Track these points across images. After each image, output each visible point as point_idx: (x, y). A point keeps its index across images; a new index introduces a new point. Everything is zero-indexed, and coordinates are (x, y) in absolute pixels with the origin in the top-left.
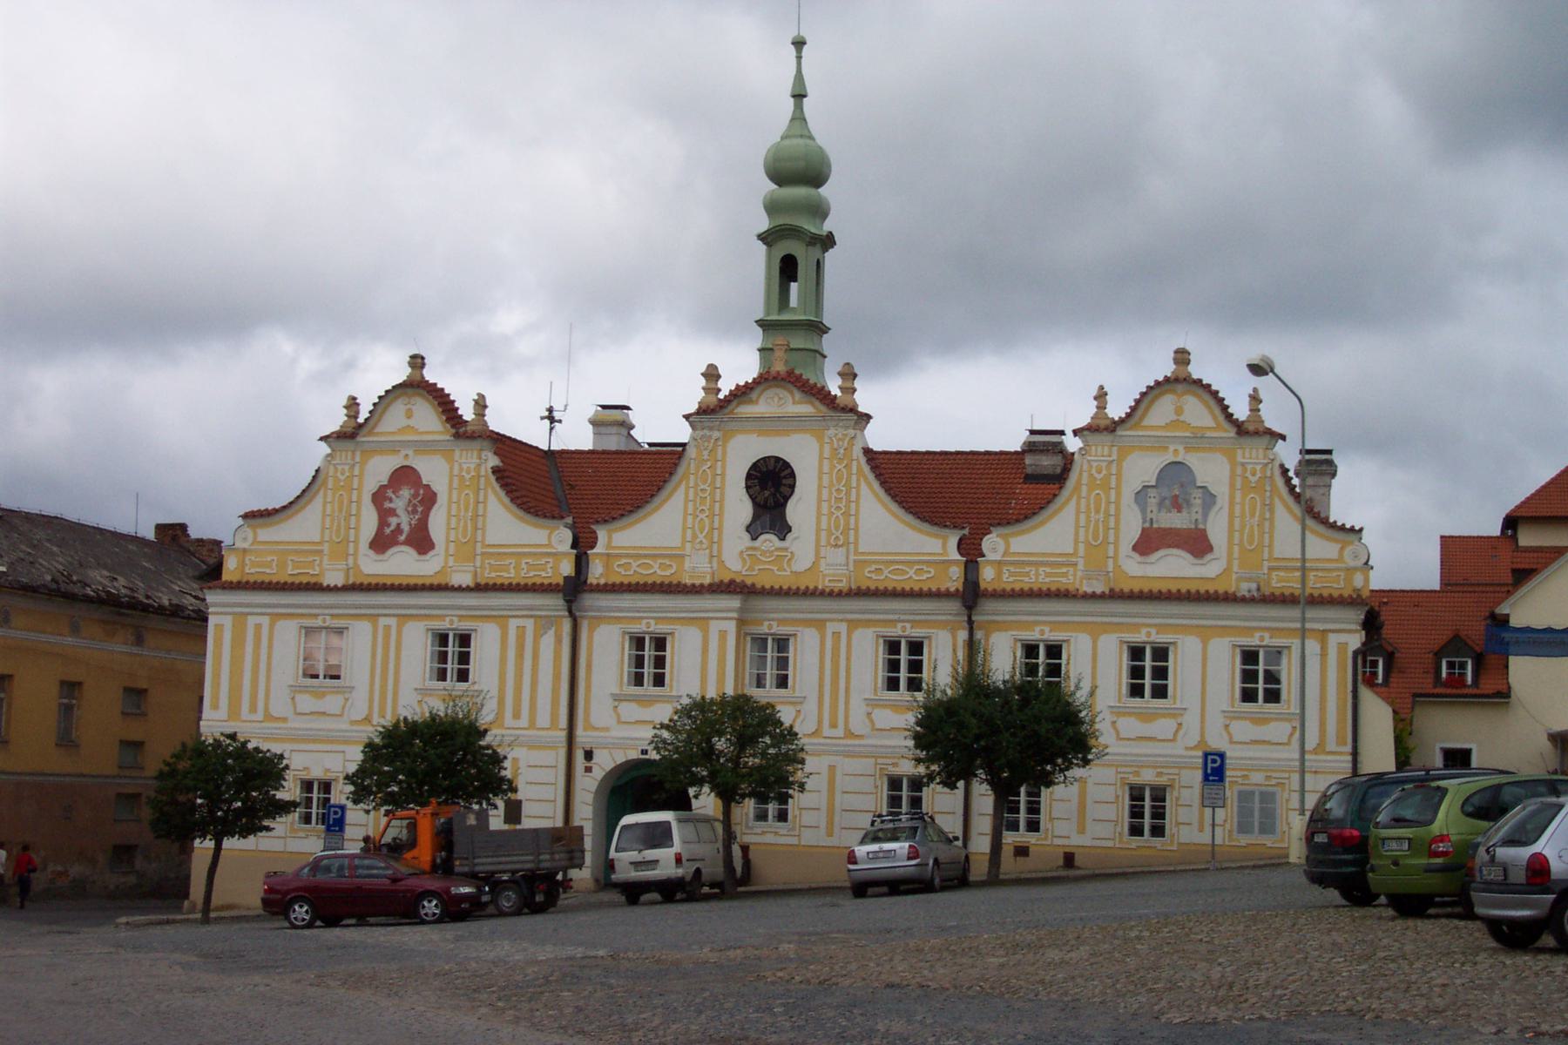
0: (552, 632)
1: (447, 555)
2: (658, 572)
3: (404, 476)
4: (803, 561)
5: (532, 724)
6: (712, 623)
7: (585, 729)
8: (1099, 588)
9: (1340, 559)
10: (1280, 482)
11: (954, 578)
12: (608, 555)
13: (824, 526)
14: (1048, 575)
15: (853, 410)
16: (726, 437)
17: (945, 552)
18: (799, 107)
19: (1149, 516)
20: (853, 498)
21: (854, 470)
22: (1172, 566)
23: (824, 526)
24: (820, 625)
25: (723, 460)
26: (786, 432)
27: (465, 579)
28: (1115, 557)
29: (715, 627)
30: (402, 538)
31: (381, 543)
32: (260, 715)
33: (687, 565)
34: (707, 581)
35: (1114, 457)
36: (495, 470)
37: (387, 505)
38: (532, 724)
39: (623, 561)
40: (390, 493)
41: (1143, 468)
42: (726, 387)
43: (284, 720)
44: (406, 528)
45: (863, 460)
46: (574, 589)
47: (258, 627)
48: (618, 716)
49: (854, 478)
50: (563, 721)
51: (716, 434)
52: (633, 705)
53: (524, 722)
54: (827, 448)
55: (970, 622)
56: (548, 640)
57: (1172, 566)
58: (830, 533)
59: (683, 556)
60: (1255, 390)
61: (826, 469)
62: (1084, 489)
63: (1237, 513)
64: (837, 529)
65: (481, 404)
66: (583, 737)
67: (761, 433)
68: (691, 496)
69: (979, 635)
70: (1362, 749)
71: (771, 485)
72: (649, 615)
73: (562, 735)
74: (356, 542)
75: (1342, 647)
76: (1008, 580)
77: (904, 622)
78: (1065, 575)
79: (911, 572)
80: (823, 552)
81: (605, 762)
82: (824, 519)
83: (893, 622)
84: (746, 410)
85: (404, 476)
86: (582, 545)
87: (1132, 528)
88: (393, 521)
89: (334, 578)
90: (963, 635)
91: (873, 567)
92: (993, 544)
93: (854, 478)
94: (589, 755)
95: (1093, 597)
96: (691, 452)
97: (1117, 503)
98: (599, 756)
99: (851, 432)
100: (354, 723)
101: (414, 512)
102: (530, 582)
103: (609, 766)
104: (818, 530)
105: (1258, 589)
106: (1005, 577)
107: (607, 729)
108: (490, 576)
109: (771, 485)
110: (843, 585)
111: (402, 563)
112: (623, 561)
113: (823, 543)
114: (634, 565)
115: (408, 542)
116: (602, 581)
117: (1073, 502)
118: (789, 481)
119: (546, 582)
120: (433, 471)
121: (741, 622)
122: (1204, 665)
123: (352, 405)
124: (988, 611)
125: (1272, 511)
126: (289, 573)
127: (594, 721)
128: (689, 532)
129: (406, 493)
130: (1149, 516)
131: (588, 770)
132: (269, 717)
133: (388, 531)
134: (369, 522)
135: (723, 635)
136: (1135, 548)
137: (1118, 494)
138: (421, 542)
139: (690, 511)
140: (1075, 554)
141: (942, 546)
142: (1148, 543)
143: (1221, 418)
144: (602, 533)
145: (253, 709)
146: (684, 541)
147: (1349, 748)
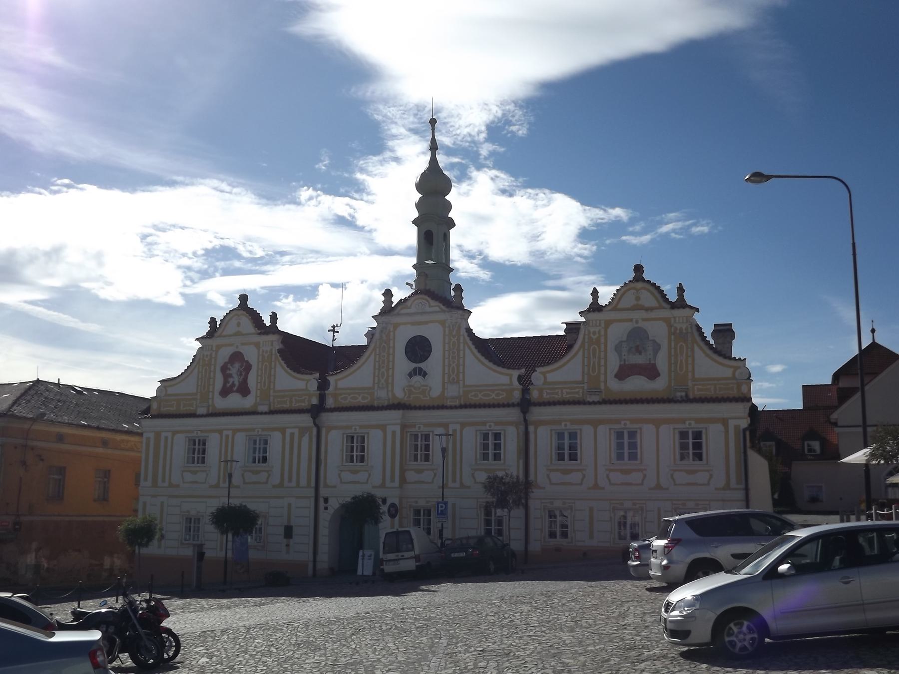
0: (307, 435)
1: (256, 396)
2: (361, 400)
3: (237, 357)
4: (436, 392)
5: (298, 485)
8: (596, 398)
9: (734, 377)
10: (696, 334)
11: (517, 395)
13: (446, 371)
14: (567, 393)
15: (461, 307)
16: (396, 326)
17: (511, 384)
19: (624, 357)
20: (462, 355)
21: (462, 341)
22: (637, 384)
23: (446, 371)
27: (264, 408)
28: (606, 382)
30: (235, 389)
31: (225, 392)
32: (166, 484)
34: (386, 403)
35: (603, 325)
36: (280, 351)
37: (228, 372)
38: (298, 485)
40: (229, 366)
41: (618, 332)
42: (395, 300)
43: (178, 486)
44: (237, 383)
45: (466, 334)
46: (317, 410)
47: (166, 438)
50: (313, 484)
53: (294, 484)
54: (447, 329)
55: (525, 420)
56: (305, 440)
57: (637, 384)
60: (680, 284)
61: (447, 341)
62: (586, 344)
63: (673, 353)
65: (274, 317)
66: (323, 492)
69: (531, 429)
70: (751, 486)
74: (213, 392)
75: (737, 427)
76: (546, 397)
78: (578, 393)
79: (494, 396)
81: (334, 504)
85: (237, 357)
87: (614, 363)
88: (231, 380)
89: (201, 411)
90: (522, 428)
92: (537, 377)
93: (462, 345)
94: (326, 500)
95: (594, 403)
97: (606, 351)
98: (330, 500)
100: (211, 487)
101: (241, 375)
103: (337, 506)
105: (687, 395)
106: (545, 395)
107: (335, 487)
108: (278, 406)
109: (418, 349)
110: (457, 403)
111: (235, 401)
113: (446, 380)
115: (237, 391)
116: (333, 406)
117: (581, 353)
120: (251, 355)
121: (404, 427)
122: (658, 442)
123: (213, 321)
124: (537, 413)
125: (693, 351)
126: (183, 409)
129: (237, 365)
130: (624, 357)
131: (326, 508)
132: (171, 485)
133: (228, 385)
134: (219, 382)
135: (394, 433)
136: (616, 376)
137: (606, 346)
138: (244, 390)
140: (582, 382)
142: (624, 373)
143: (661, 300)
145: (163, 481)
147: (743, 486)
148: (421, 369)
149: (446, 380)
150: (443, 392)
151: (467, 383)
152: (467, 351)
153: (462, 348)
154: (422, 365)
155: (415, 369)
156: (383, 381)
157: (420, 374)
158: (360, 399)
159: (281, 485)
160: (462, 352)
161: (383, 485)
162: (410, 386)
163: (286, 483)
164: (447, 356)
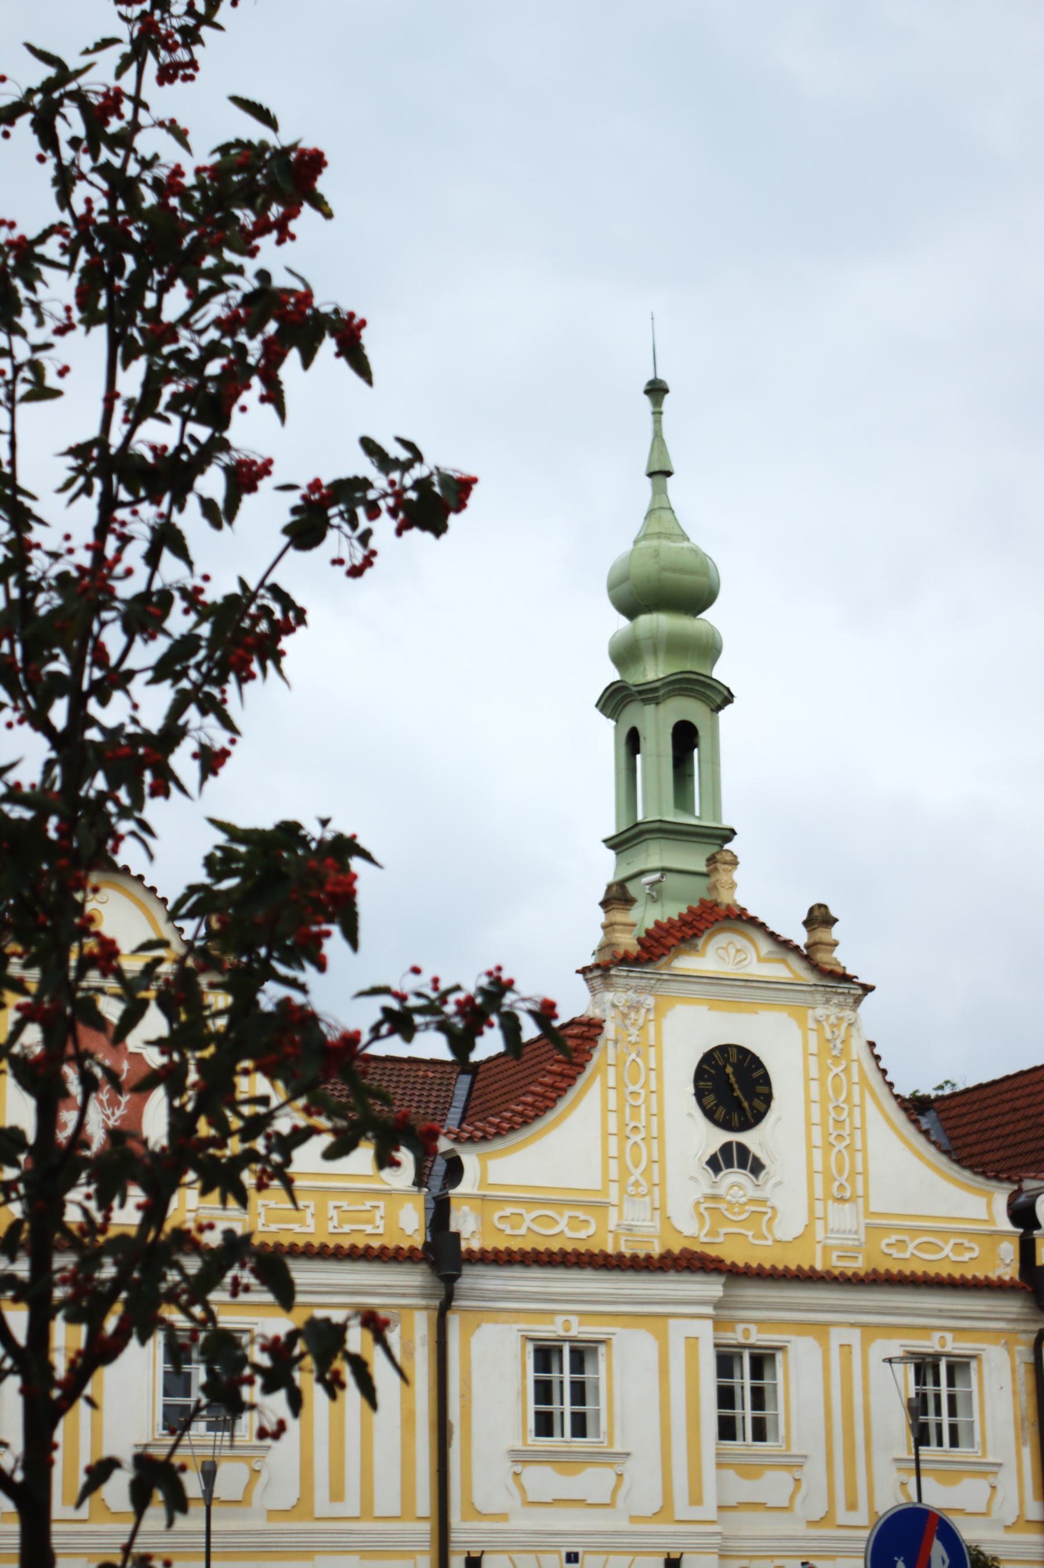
2: (565, 1232)
4: (790, 1224)
5: (367, 1511)
6: (672, 1322)
7: (464, 1518)
12: (483, 1198)
18: (660, 492)
21: (856, 1078)
23: (818, 1165)
24: (820, 1330)
25: (658, 1045)
26: (753, 1007)
29: (678, 1330)
33: (613, 1219)
34: (656, 1250)
38: (367, 1511)
39: (509, 1210)
48: (522, 1489)
49: (856, 1089)
50: (424, 1502)
51: (650, 1001)
52: (547, 1471)
53: (351, 1506)
54: (813, 1037)
58: (829, 1179)
59: (605, 1205)
64: (840, 1172)
67: (714, 1004)
68: (612, 1104)
71: (733, 1087)
72: (567, 1308)
73: (424, 1530)
77: (940, 1326)
79: (947, 1250)
80: (819, 1206)
82: (817, 1154)
83: (927, 1330)
84: (685, 963)
86: (440, 1177)
91: (893, 1239)
93: (856, 1089)
96: (610, 1030)
99: (847, 1013)
102: (346, 1243)
104: (811, 1173)
107: (504, 1517)
109: (733, 1087)
110: (858, 1265)
112: (509, 1210)
114: (529, 1217)
118: (760, 1089)
119: (376, 1244)
127: (480, 1500)
128: (613, 1165)
139: (613, 1128)
141: (986, 1205)
144: (470, 1159)
146: (606, 1180)
148: (743, 1150)
149: (819, 1193)
150: (809, 1227)
151: (873, 1208)
152: (871, 1107)
153: (857, 1100)
154: (745, 1138)
155: (726, 1148)
156: (636, 1174)
157: (742, 1165)
158: (562, 1225)
159: (303, 1507)
160: (857, 1111)
161: (665, 1512)
162: (715, 1198)
163: (322, 1504)
164: (816, 1118)
